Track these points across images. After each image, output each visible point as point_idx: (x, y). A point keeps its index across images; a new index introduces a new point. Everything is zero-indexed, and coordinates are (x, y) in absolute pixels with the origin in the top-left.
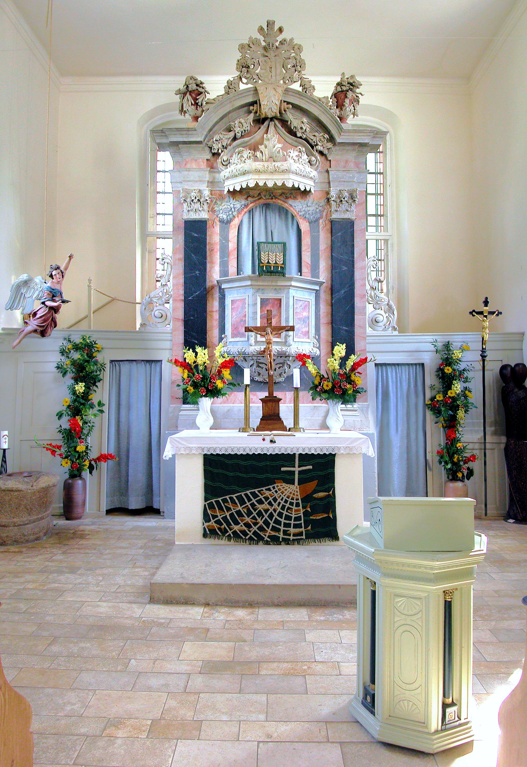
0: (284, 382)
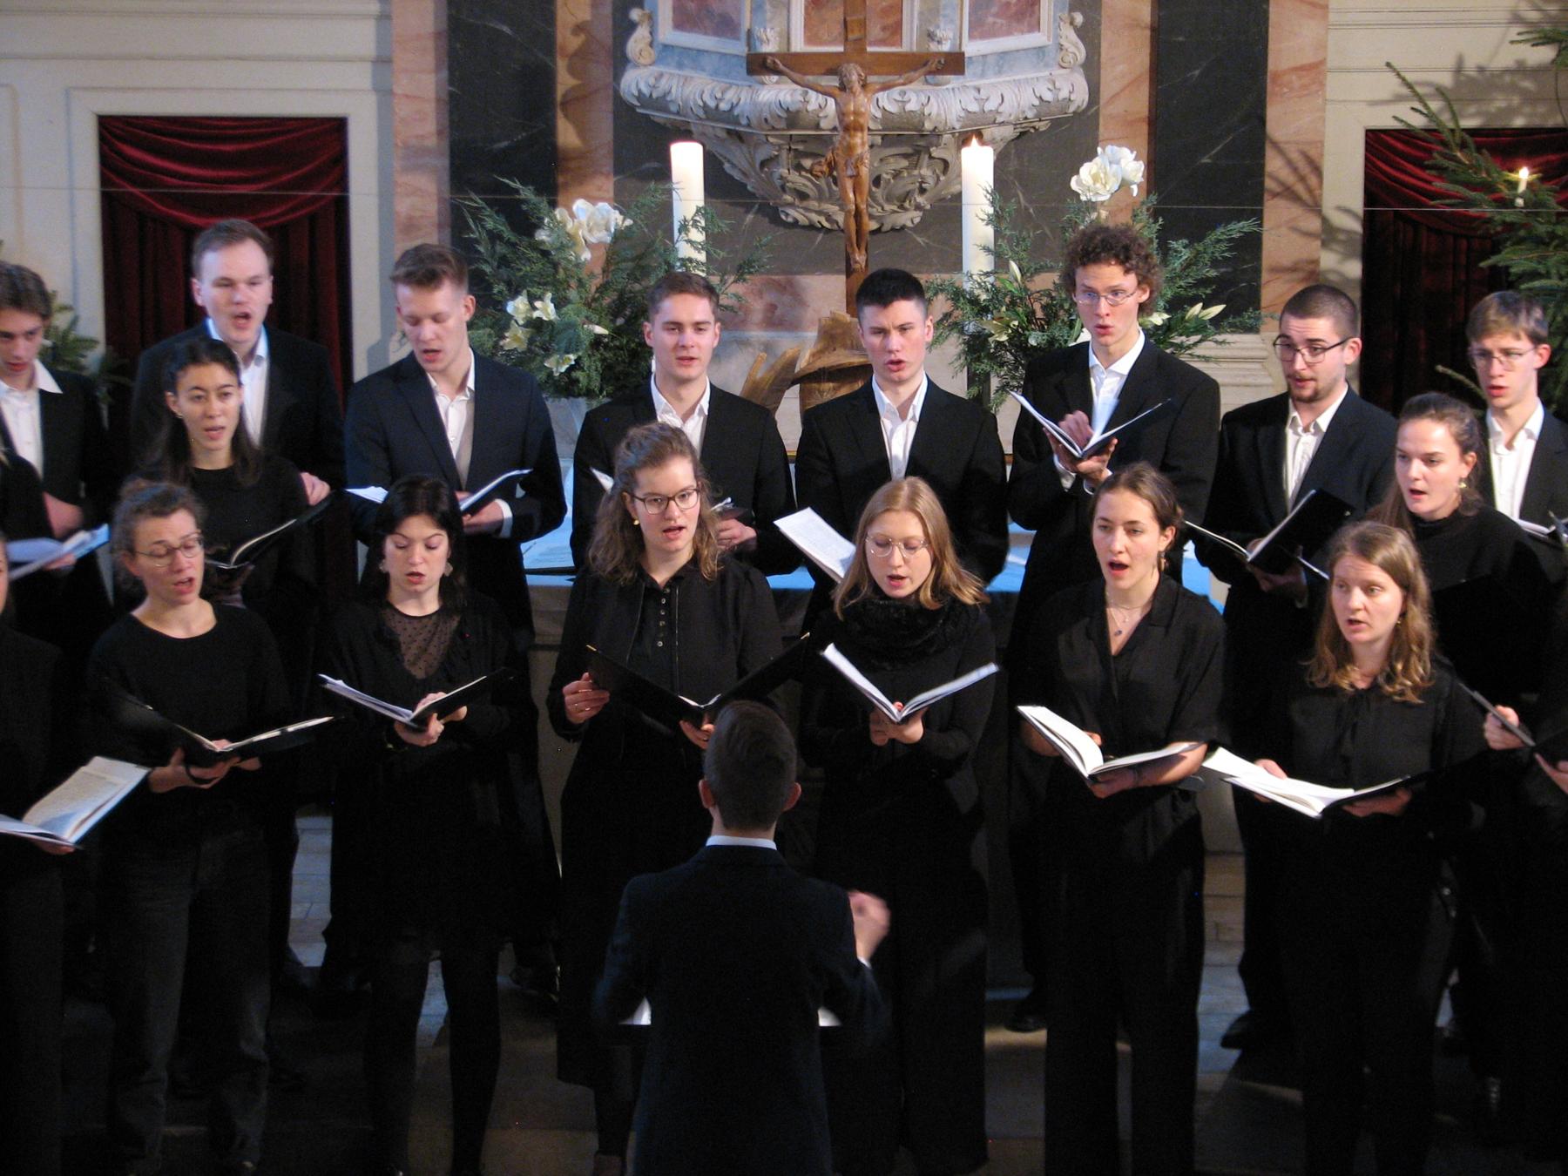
0: (920, 228)
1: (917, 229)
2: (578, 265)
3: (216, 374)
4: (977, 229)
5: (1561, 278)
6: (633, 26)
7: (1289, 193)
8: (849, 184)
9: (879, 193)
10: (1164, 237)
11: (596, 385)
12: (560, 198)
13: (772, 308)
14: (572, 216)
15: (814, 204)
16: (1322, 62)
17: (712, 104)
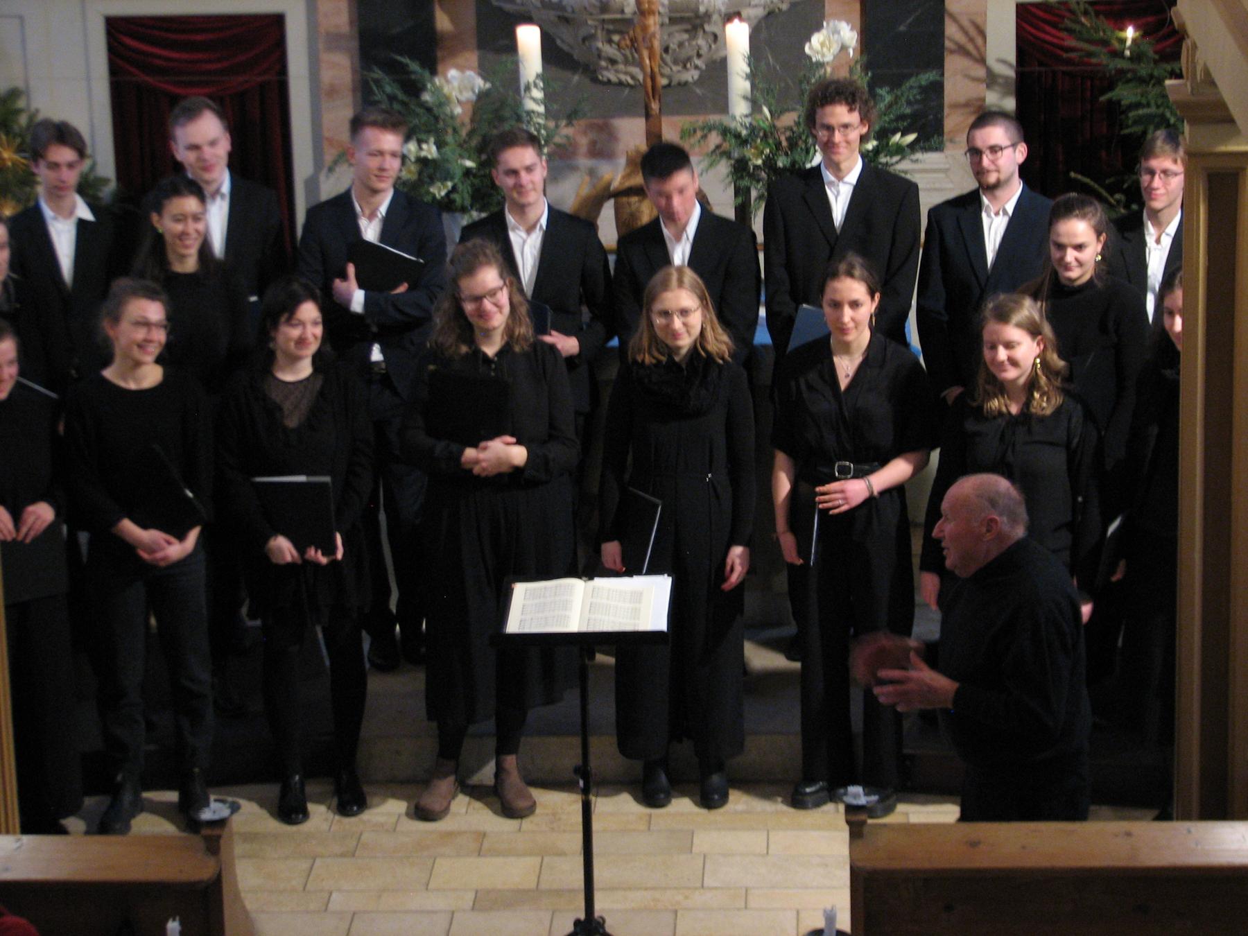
1: (695, 83)
2: (452, 117)
3: (190, 204)
4: (739, 82)
5: (1158, 107)
7: (962, 50)
8: (645, 54)
9: (668, 58)
10: (872, 85)
11: (468, 202)
12: (440, 68)
13: (593, 143)
14: (448, 81)
15: (621, 67)
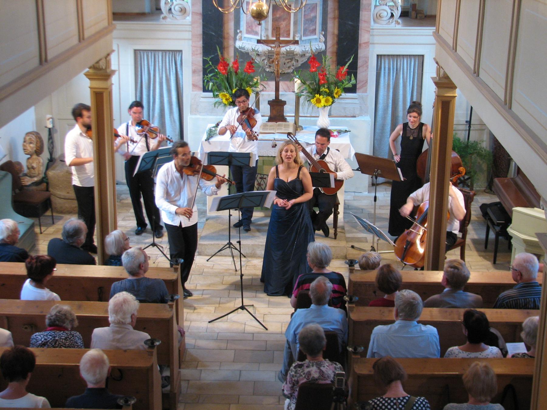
6: (238, 33)
16: (369, 42)
17: (254, 49)
